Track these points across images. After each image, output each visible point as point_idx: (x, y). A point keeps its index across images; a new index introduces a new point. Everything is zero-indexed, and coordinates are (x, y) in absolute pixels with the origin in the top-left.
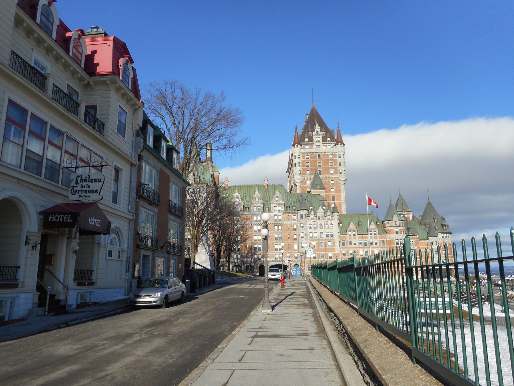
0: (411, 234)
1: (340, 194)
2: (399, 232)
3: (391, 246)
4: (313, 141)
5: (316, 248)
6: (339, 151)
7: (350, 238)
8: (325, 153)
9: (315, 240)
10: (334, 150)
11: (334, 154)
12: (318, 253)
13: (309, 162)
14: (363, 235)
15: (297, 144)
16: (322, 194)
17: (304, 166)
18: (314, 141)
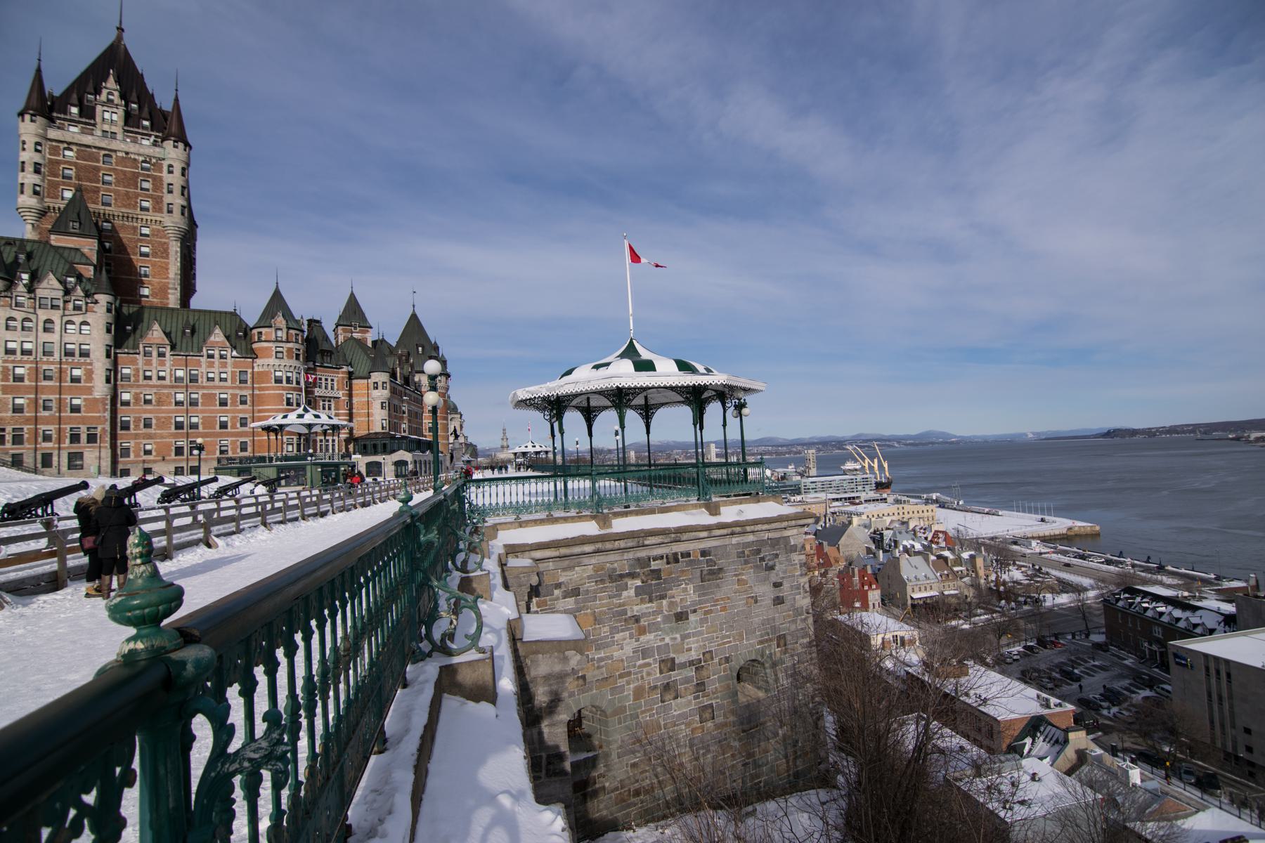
0: (330, 363)
1: (167, 264)
2: (285, 354)
3: (263, 385)
4: (93, 117)
5: (27, 382)
6: (170, 156)
7: (149, 363)
8: (127, 153)
9: (26, 362)
10: (157, 151)
11: (154, 161)
12: (33, 396)
13: (73, 168)
14: (188, 358)
15: (31, 112)
16: (85, 250)
17: (56, 175)
18: (98, 119)
